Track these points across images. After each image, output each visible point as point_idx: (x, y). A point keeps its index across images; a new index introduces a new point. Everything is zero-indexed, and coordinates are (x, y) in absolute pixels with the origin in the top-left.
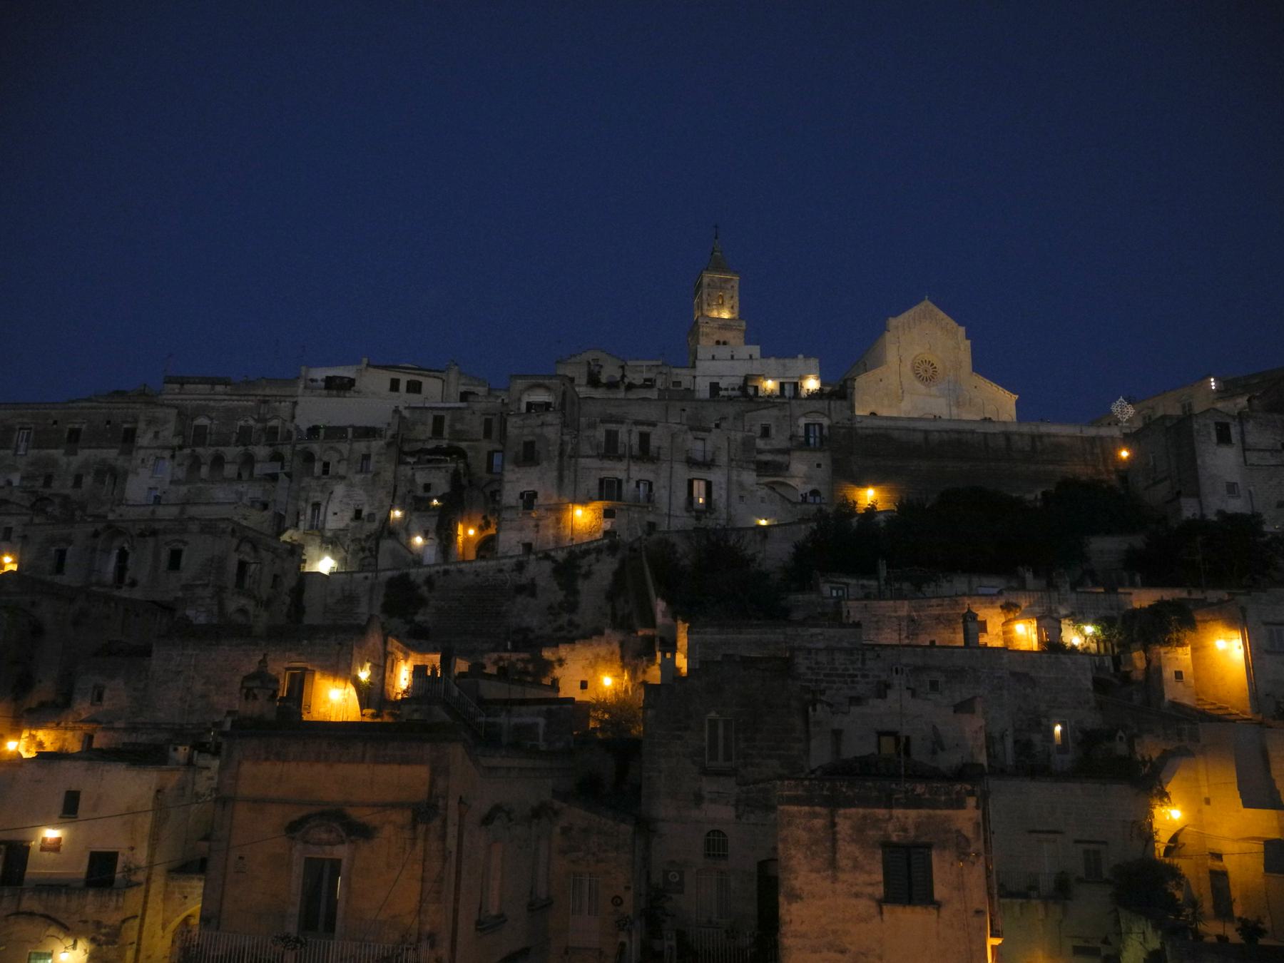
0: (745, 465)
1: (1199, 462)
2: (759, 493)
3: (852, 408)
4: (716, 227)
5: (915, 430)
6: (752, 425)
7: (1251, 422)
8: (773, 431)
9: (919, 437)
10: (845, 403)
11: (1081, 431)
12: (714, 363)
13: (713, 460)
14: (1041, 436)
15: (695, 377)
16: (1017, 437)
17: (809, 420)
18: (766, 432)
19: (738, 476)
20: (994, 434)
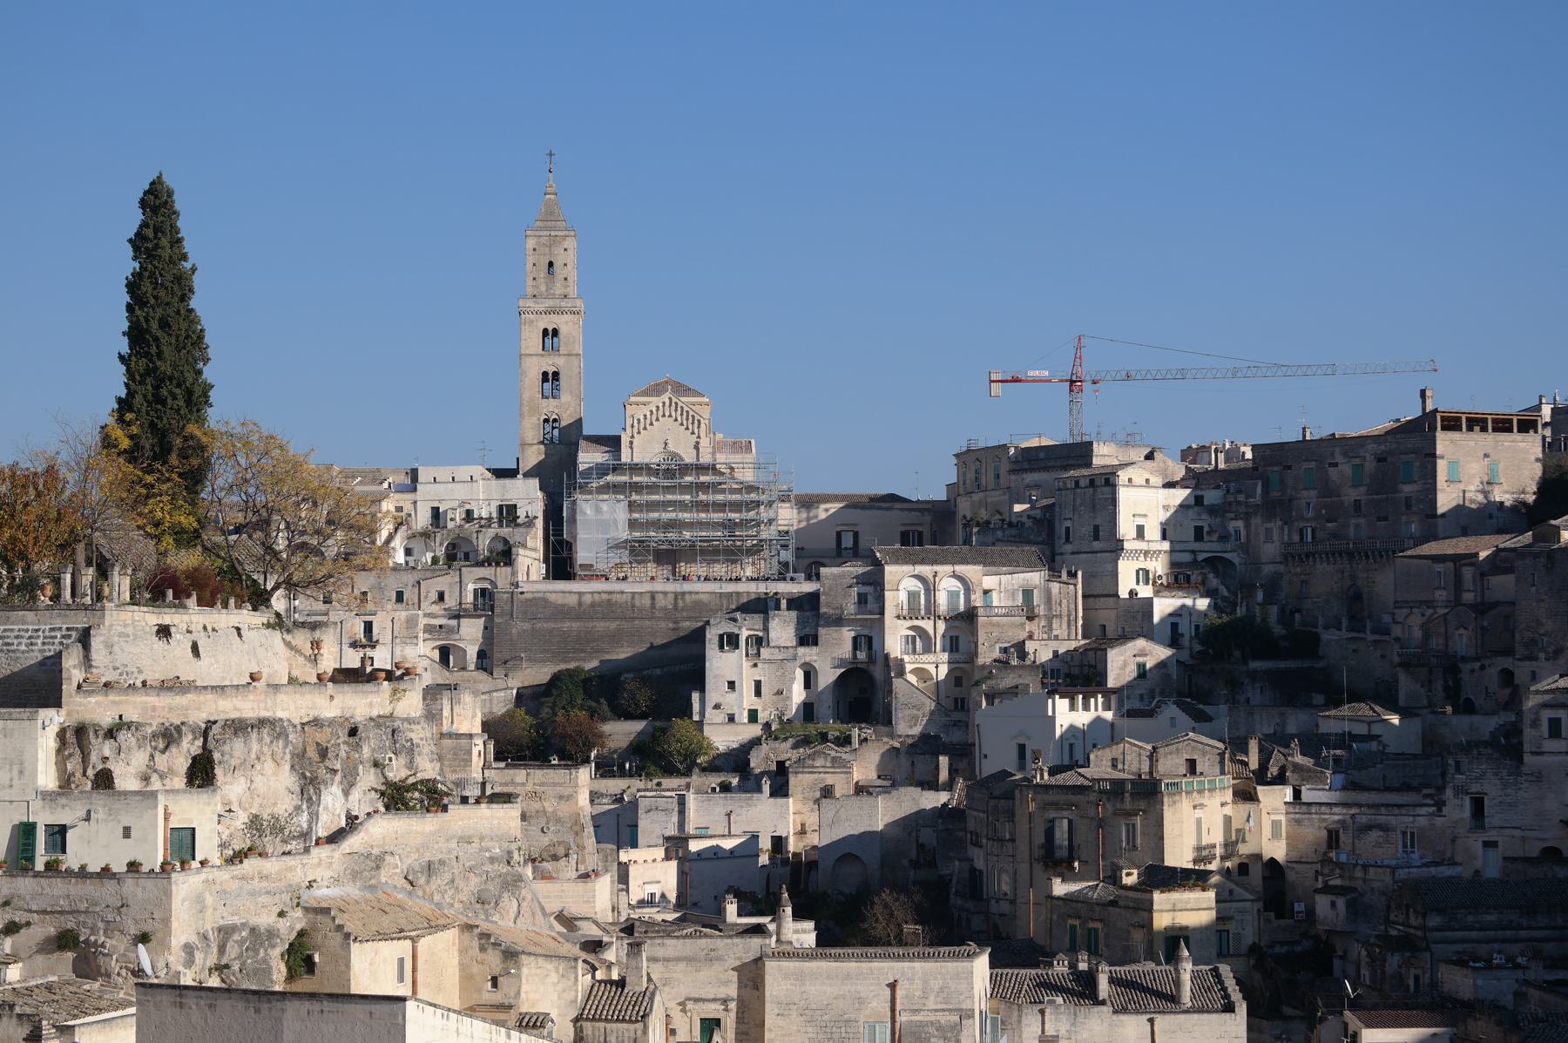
0: (408, 641)
1: (707, 665)
2: (420, 665)
3: (514, 574)
4: (551, 154)
5: (570, 592)
6: (428, 592)
7: (777, 619)
8: (446, 597)
9: (572, 600)
10: (509, 569)
11: (721, 588)
12: (437, 486)
13: (377, 641)
14: (683, 594)
15: (415, 502)
16: (661, 596)
17: (479, 586)
18: (441, 597)
19: (402, 651)
20: (641, 593)
